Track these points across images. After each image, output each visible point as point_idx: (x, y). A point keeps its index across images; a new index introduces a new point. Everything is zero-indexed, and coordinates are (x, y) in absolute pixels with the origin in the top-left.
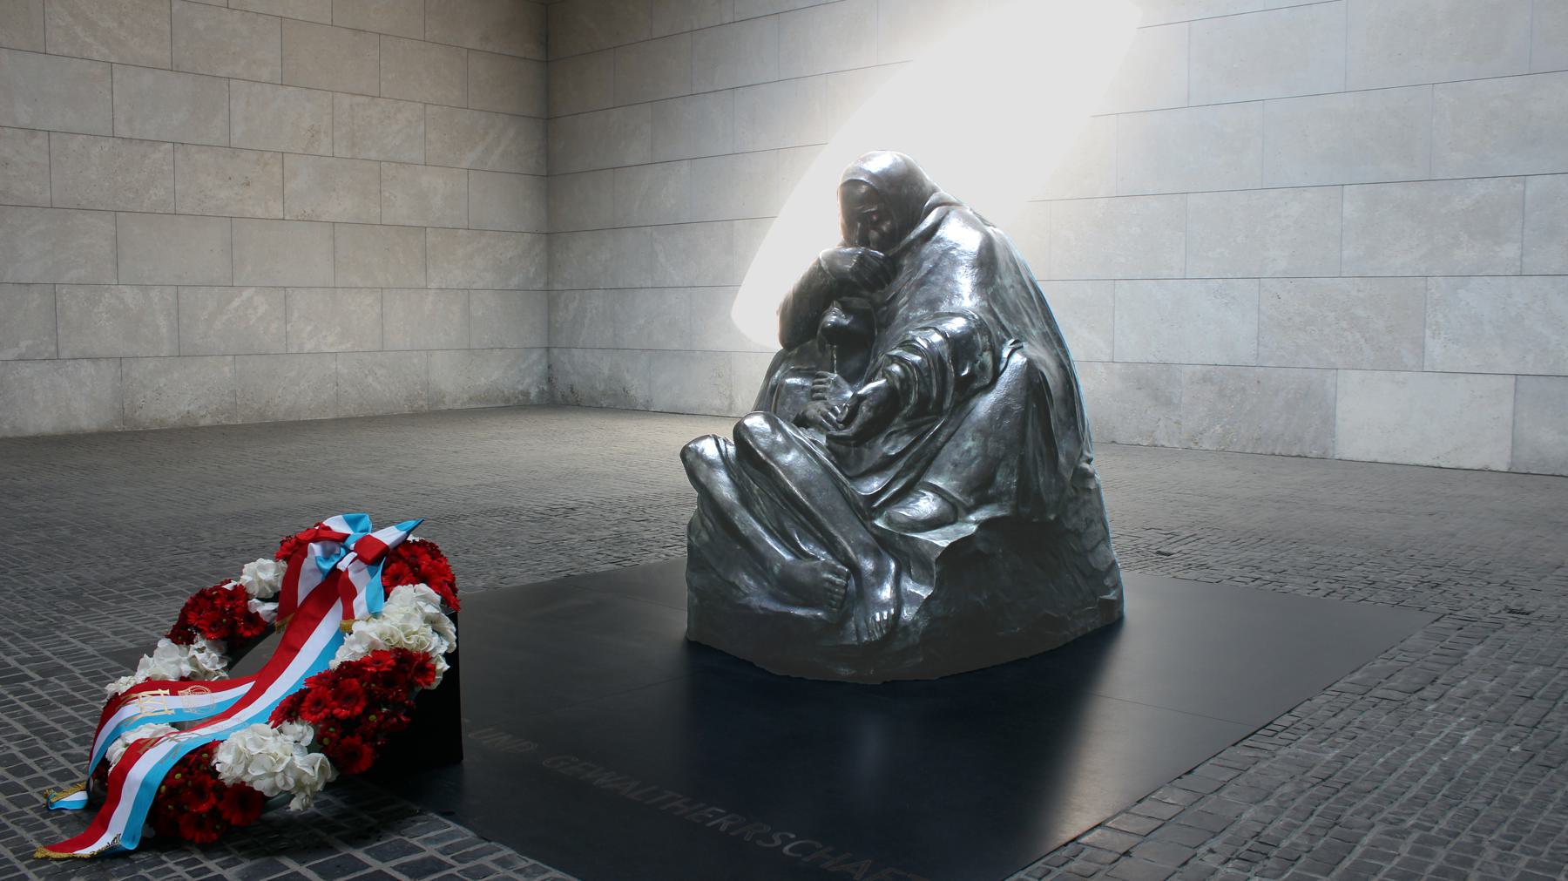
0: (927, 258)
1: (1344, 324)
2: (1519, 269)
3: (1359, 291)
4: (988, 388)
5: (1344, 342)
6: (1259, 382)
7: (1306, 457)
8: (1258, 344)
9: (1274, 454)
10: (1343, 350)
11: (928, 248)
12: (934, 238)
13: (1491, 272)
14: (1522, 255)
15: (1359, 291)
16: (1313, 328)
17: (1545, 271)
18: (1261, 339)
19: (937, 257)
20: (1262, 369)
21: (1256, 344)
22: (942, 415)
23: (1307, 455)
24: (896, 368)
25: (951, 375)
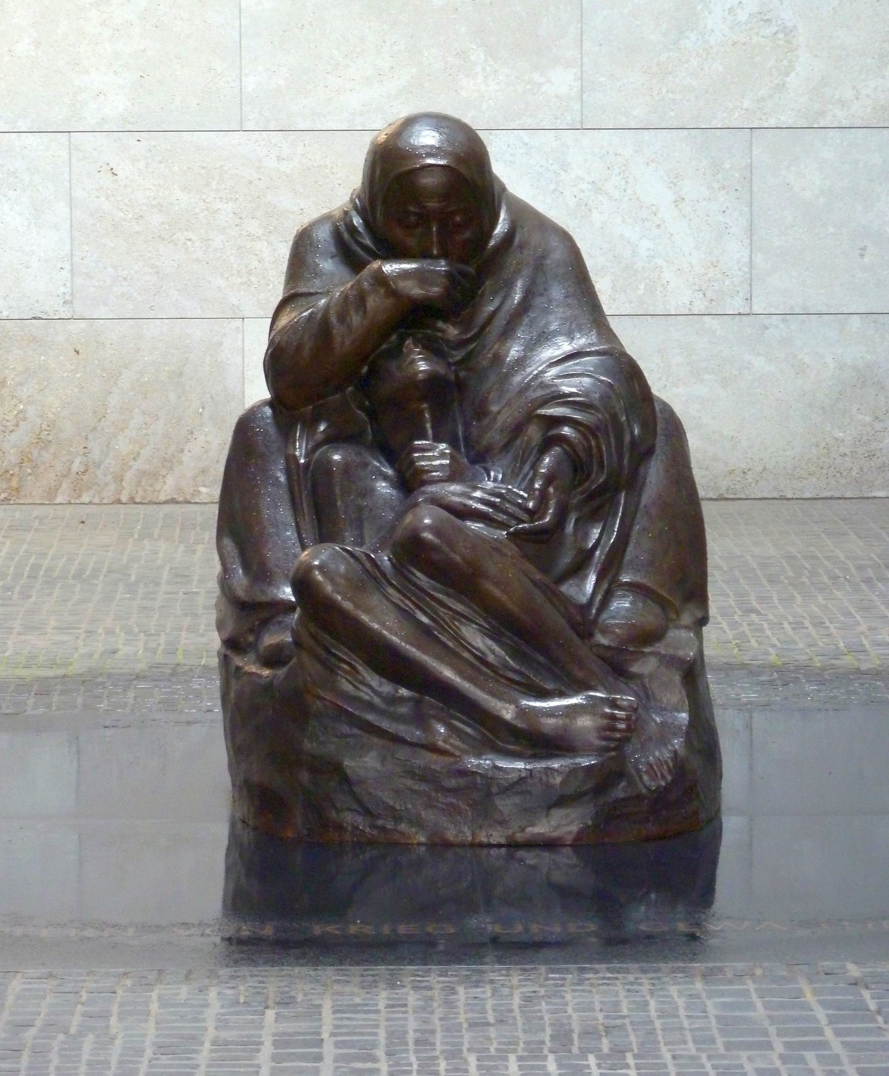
0: (517, 271)
1: (253, 227)
2: (578, 119)
3: (279, 159)
4: (650, 452)
5: (255, 263)
6: (78, 353)
7: (190, 503)
8: (72, 271)
9: (119, 502)
10: (253, 279)
11: (512, 260)
12: (517, 240)
13: (530, 122)
14: (582, 91)
15: (279, 159)
16: (190, 235)
17: (623, 121)
18: (76, 259)
19: (527, 272)
20: (82, 324)
21: (66, 274)
22: (617, 491)
23: (188, 497)
24: (566, 431)
25: (627, 438)
